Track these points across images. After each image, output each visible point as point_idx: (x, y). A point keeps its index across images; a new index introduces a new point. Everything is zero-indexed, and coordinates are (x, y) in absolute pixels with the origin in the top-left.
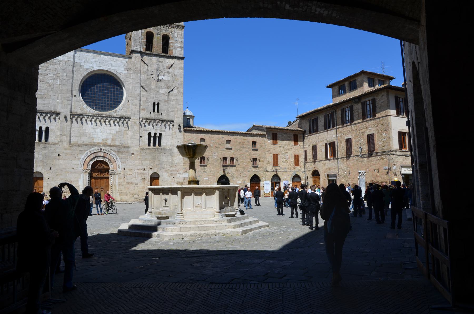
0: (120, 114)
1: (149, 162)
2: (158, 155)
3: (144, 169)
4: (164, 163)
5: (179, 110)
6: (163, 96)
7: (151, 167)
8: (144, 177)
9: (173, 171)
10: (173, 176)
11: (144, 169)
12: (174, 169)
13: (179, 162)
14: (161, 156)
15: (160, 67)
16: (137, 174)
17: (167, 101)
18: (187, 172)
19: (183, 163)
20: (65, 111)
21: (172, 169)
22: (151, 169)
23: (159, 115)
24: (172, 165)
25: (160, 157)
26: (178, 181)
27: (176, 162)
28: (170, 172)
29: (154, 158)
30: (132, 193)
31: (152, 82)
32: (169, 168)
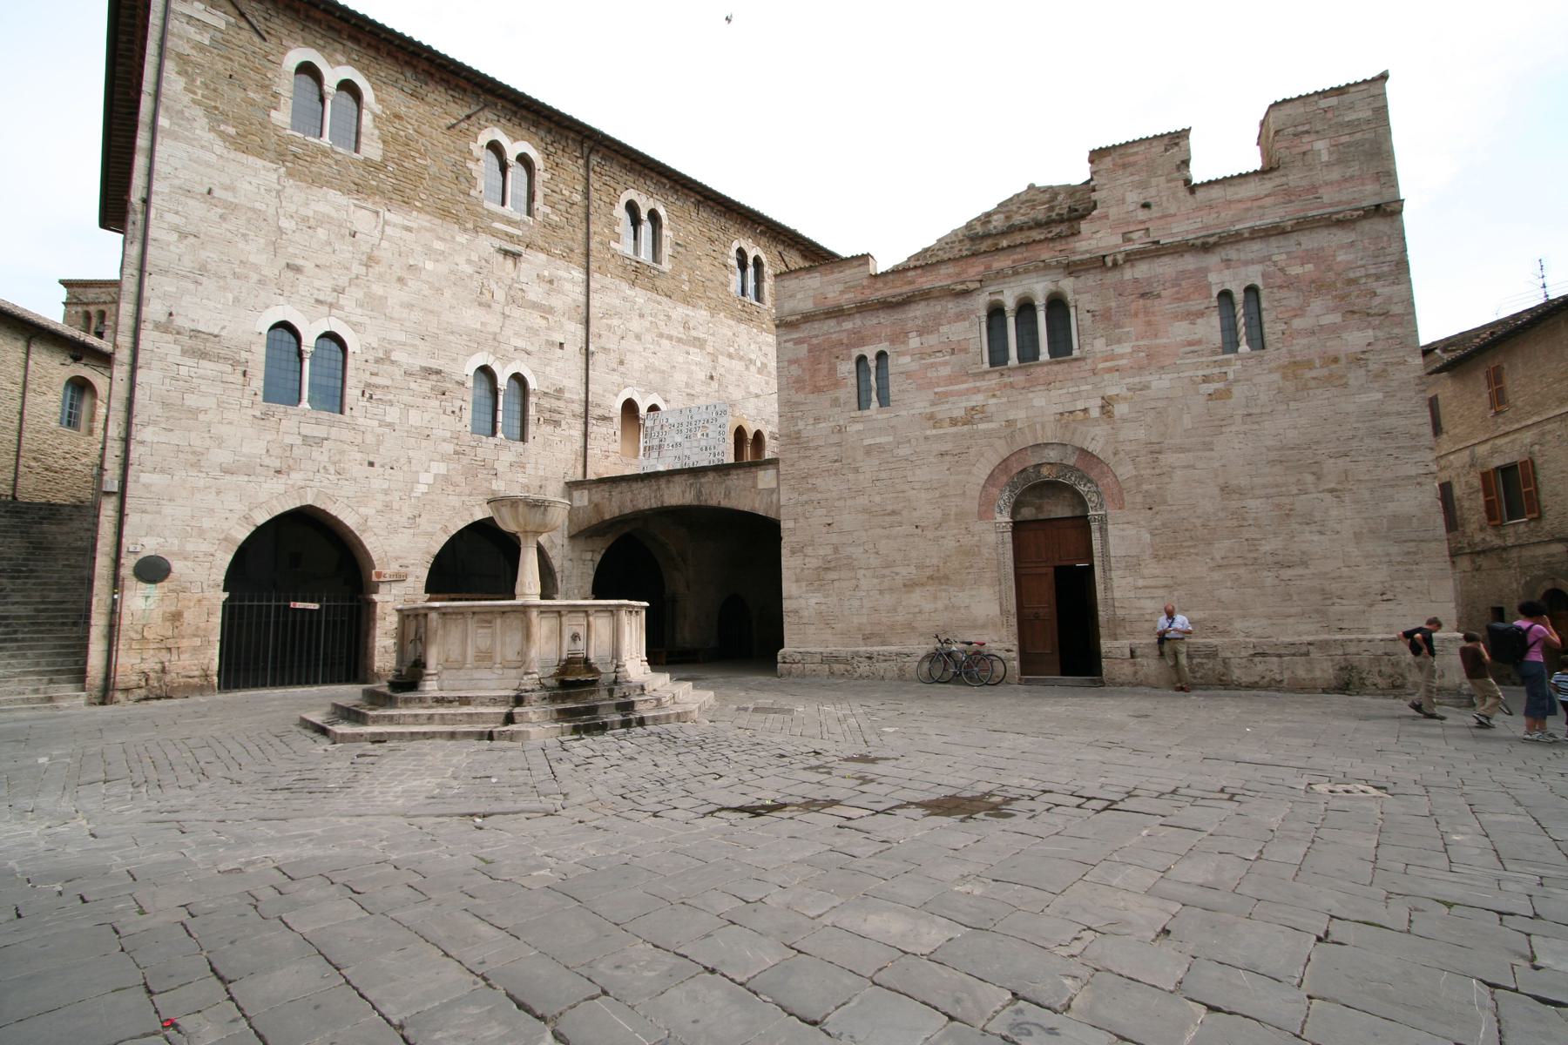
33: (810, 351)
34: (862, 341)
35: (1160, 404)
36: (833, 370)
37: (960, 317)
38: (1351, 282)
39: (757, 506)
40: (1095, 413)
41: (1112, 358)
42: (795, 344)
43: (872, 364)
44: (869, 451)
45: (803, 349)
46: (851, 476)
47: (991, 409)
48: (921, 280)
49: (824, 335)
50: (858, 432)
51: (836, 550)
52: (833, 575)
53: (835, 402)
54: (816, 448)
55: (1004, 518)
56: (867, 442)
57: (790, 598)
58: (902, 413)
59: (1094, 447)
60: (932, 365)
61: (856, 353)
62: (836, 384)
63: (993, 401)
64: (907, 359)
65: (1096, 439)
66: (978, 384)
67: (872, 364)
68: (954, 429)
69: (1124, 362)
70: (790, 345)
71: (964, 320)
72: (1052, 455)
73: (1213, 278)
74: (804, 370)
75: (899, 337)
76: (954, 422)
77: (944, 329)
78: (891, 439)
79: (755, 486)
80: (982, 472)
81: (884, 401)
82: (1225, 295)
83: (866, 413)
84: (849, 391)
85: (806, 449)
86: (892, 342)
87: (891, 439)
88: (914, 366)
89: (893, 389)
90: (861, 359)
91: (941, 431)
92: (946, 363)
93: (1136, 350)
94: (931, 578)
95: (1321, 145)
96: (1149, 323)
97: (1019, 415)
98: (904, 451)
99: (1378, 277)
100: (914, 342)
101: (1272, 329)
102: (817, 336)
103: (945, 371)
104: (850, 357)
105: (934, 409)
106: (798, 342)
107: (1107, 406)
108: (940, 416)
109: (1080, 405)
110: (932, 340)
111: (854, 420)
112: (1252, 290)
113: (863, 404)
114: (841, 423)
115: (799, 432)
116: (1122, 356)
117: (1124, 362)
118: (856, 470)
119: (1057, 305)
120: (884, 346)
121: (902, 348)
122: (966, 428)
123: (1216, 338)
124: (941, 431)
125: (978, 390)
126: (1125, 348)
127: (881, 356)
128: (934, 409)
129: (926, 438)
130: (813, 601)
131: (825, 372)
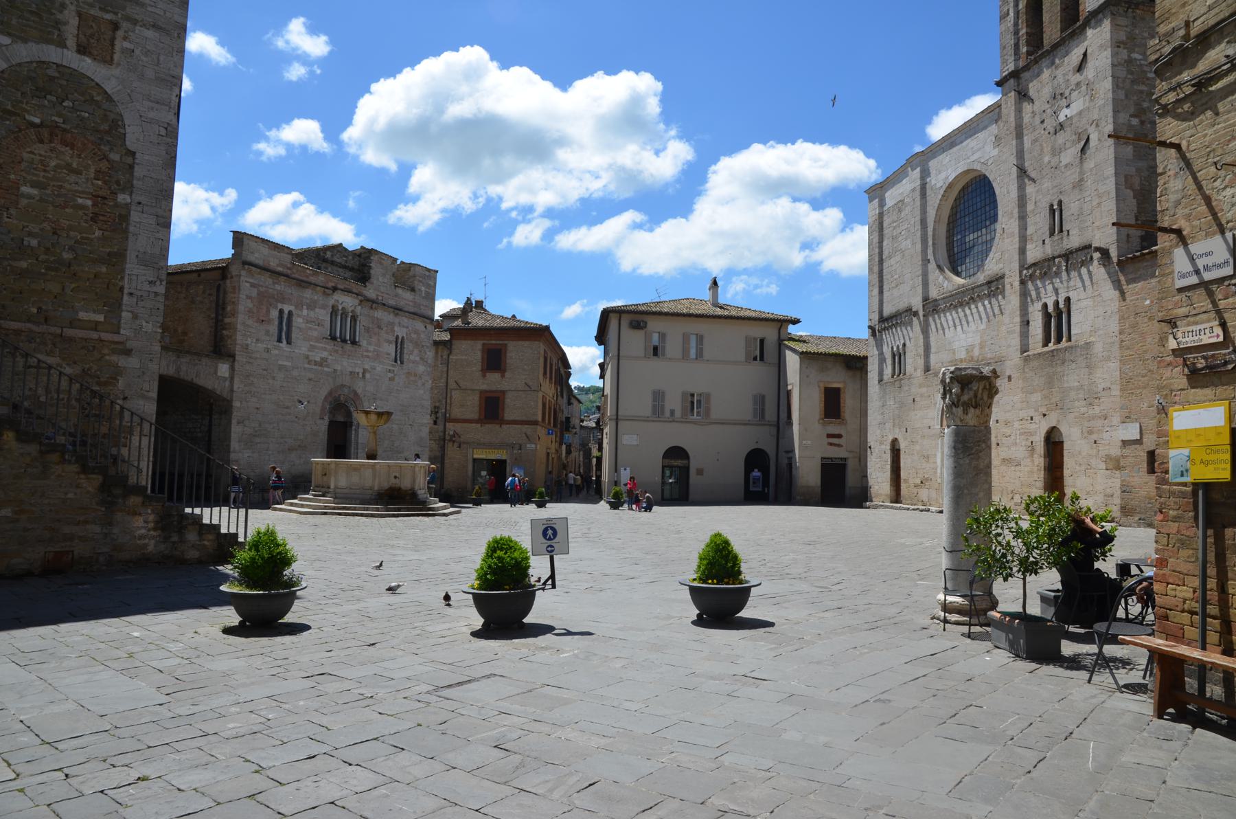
0: (990, 272)
1: (1039, 394)
2: (1059, 369)
3: (1032, 419)
4: (1073, 394)
5: (1104, 199)
6: (1069, 173)
7: (1043, 410)
8: (1032, 442)
9: (1093, 418)
10: (1094, 437)
11: (1032, 419)
12: (1097, 410)
13: (1108, 385)
14: (1066, 373)
15: (1059, 85)
16: (1018, 432)
17: (1079, 185)
18: (1130, 418)
19: (1119, 387)
20: (917, 303)
21: (1091, 412)
22: (1044, 415)
23: (1062, 238)
24: (1092, 398)
25: (1063, 375)
26: (1106, 452)
27: (1101, 387)
28: (1086, 424)
29: (1050, 382)
30: (1010, 489)
31: (1045, 145)
32: (1083, 410)
33: (258, 294)
34: (283, 299)
35: (377, 378)
36: (268, 312)
37: (324, 307)
38: (423, 346)
39: (216, 387)
40: (361, 375)
41: (367, 351)
42: (251, 286)
43: (285, 316)
44: (281, 368)
45: (254, 292)
46: (271, 381)
47: (329, 361)
48: (312, 278)
49: (266, 287)
50: (276, 355)
51: (260, 425)
52: (258, 440)
53: (267, 333)
54: (256, 358)
55: (327, 419)
56: (280, 363)
57: (234, 452)
58: (296, 351)
59: (359, 391)
60: (310, 328)
61: (280, 306)
62: (269, 321)
63: (330, 357)
64: (300, 320)
65: (359, 387)
66: (327, 346)
67: (285, 316)
68: (315, 367)
69: (370, 354)
70: (248, 285)
71: (325, 309)
72: (346, 390)
73: (396, 329)
74: (254, 305)
75: (299, 306)
76: (316, 363)
77: (317, 310)
78: (289, 364)
79: (216, 373)
80: (324, 392)
81: (289, 342)
82: (397, 337)
83: (280, 344)
84: (274, 328)
85: (251, 358)
86: (296, 307)
87: (289, 364)
88: (303, 326)
89: (294, 336)
90: (281, 312)
91: (311, 367)
92: (316, 330)
93: (374, 351)
94: (299, 446)
95: (423, 289)
96: (379, 340)
97: (339, 368)
98: (295, 373)
99: (427, 347)
100: (305, 312)
101: (406, 357)
102: (262, 286)
103: (315, 334)
104: (276, 308)
105: (310, 353)
106: (253, 285)
107: (365, 371)
108: (311, 358)
109: (357, 370)
110: (312, 314)
111: (276, 347)
112: (403, 338)
113: (279, 340)
114: (269, 347)
115: (247, 345)
116: (370, 351)
117: (370, 354)
118: (274, 378)
119: (354, 319)
120: (292, 308)
121: (300, 313)
122: (320, 368)
123: (393, 354)
124: (311, 367)
125: (325, 349)
126: (371, 348)
127: (290, 313)
128: (310, 353)
129: (305, 368)
130: (246, 455)
131: (264, 311)
